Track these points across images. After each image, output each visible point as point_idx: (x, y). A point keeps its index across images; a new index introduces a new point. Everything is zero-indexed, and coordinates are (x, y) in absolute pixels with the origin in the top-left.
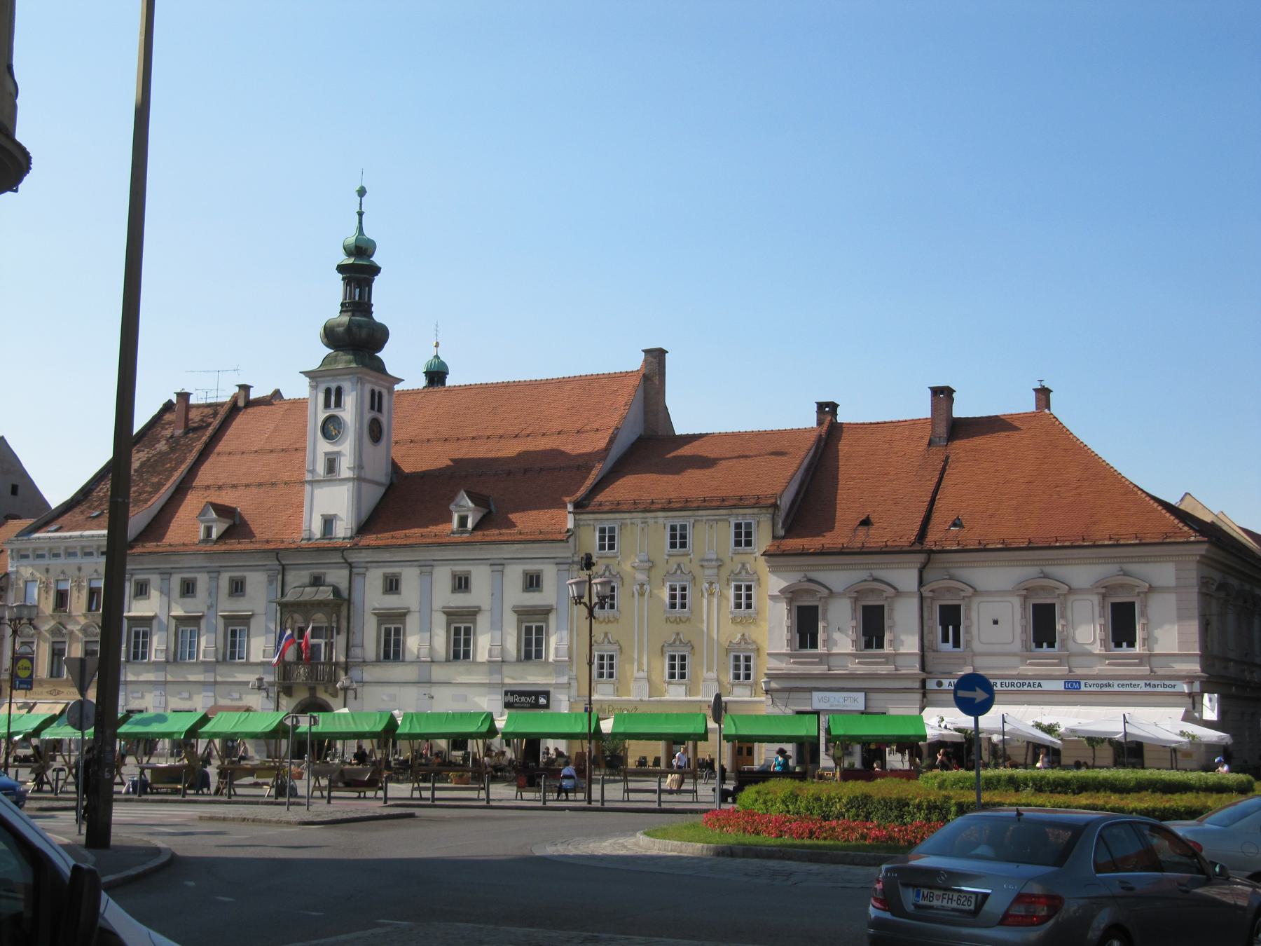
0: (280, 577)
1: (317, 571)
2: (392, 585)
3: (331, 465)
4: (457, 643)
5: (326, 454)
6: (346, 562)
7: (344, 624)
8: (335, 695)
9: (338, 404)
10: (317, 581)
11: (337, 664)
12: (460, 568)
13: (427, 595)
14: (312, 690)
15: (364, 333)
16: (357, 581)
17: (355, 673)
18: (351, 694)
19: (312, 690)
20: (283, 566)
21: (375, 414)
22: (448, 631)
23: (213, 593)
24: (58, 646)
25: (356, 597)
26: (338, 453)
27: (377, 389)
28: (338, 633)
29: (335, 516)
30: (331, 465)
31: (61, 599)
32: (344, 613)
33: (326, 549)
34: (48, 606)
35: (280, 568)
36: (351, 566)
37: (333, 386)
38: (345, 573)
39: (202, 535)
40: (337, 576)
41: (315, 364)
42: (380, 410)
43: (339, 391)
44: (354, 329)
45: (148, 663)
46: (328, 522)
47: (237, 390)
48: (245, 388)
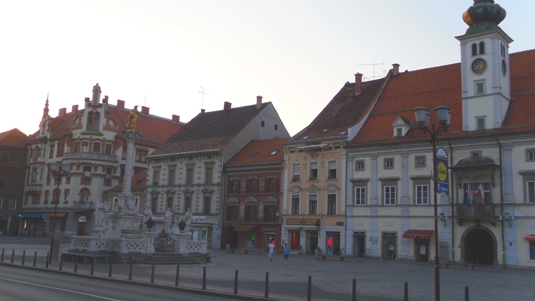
3: (480, 87)
5: (475, 81)
6: (499, 143)
7: (497, 181)
8: (494, 225)
9: (482, 52)
10: (476, 155)
11: (495, 205)
14: (477, 221)
15: (495, 10)
16: (505, 154)
17: (507, 210)
18: (506, 224)
20: (452, 149)
21: (504, 58)
23: (404, 166)
24: (313, 199)
25: (505, 164)
26: (484, 80)
27: (503, 44)
28: (494, 187)
29: (486, 116)
30: (480, 87)
31: (314, 173)
32: (497, 174)
33: (482, 135)
34: (305, 176)
35: (449, 150)
36: (500, 146)
37: (478, 42)
38: (496, 150)
39: (395, 134)
40: (490, 153)
41: (463, 33)
42: (504, 56)
43: (482, 45)
44: (489, 8)
45: (366, 206)
47: (392, 67)
48: (396, 66)
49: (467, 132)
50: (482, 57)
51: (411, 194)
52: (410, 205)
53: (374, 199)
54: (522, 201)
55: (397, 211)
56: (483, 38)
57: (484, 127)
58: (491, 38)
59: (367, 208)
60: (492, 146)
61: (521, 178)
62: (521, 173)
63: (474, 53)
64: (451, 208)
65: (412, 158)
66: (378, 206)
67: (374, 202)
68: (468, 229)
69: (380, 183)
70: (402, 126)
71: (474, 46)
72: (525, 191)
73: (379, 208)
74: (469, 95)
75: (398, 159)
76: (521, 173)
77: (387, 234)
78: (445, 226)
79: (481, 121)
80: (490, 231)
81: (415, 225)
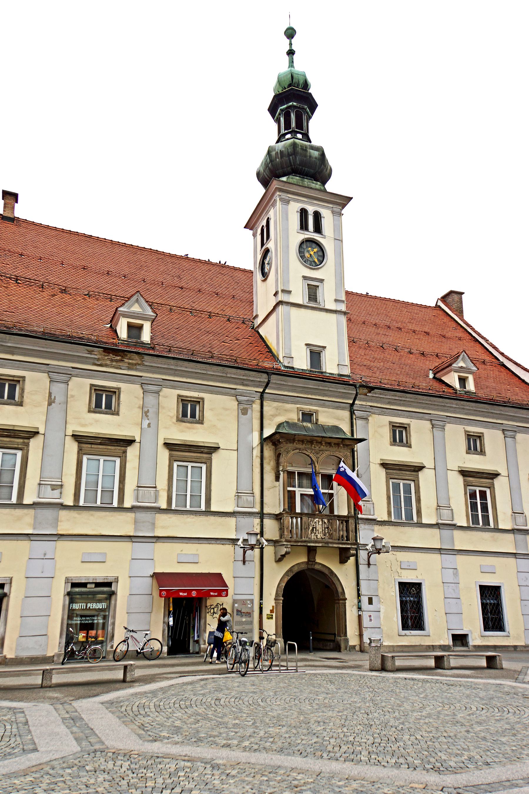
0: (256, 406)
1: (308, 408)
2: (399, 435)
4: (474, 506)
5: (305, 278)
9: (318, 229)
10: (307, 416)
12: (474, 429)
13: (439, 451)
16: (359, 424)
19: (311, 551)
22: (466, 493)
26: (322, 281)
29: (325, 347)
38: (346, 414)
40: (332, 417)
43: (317, 216)
46: (316, 354)
49: (293, 368)
50: (316, 237)
51: (162, 484)
52: (159, 510)
53: (54, 488)
54: (386, 518)
55: (123, 524)
56: (323, 207)
57: (320, 367)
58: (333, 212)
59: (19, 512)
60: (338, 406)
61: (382, 472)
62: (384, 465)
63: (304, 226)
64: (257, 521)
65: (170, 399)
66: (63, 506)
67: (51, 497)
68: (290, 570)
69: (72, 447)
70: (145, 319)
71: (303, 213)
72: (389, 498)
73: (63, 513)
74: (292, 299)
75: (130, 394)
76: (384, 465)
77: (84, 585)
78: (244, 562)
79: (316, 354)
80: (332, 572)
81: (170, 560)
